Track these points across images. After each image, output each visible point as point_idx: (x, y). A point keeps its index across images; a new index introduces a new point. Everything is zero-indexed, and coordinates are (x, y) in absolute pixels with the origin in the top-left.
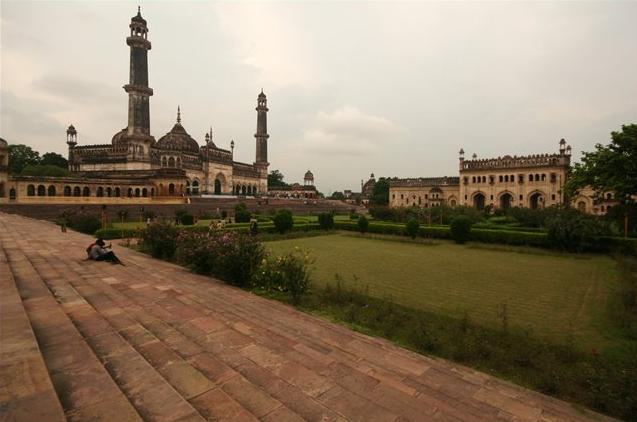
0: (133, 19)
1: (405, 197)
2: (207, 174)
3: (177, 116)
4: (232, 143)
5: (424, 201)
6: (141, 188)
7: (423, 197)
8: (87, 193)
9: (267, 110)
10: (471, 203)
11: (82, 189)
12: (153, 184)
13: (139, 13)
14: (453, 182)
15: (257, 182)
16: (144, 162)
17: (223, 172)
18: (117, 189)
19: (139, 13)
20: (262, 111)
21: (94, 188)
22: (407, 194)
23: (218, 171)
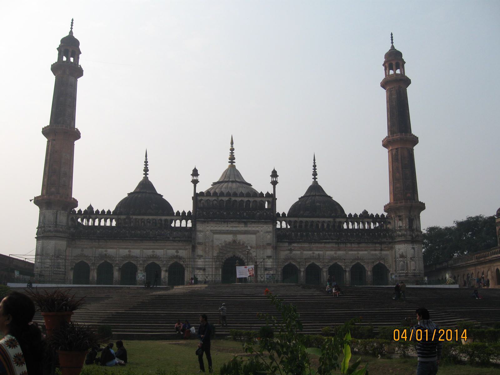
2: (194, 248)
3: (228, 155)
4: (274, 174)
13: (71, 32)
17: (240, 237)
19: (71, 32)
23: (229, 238)
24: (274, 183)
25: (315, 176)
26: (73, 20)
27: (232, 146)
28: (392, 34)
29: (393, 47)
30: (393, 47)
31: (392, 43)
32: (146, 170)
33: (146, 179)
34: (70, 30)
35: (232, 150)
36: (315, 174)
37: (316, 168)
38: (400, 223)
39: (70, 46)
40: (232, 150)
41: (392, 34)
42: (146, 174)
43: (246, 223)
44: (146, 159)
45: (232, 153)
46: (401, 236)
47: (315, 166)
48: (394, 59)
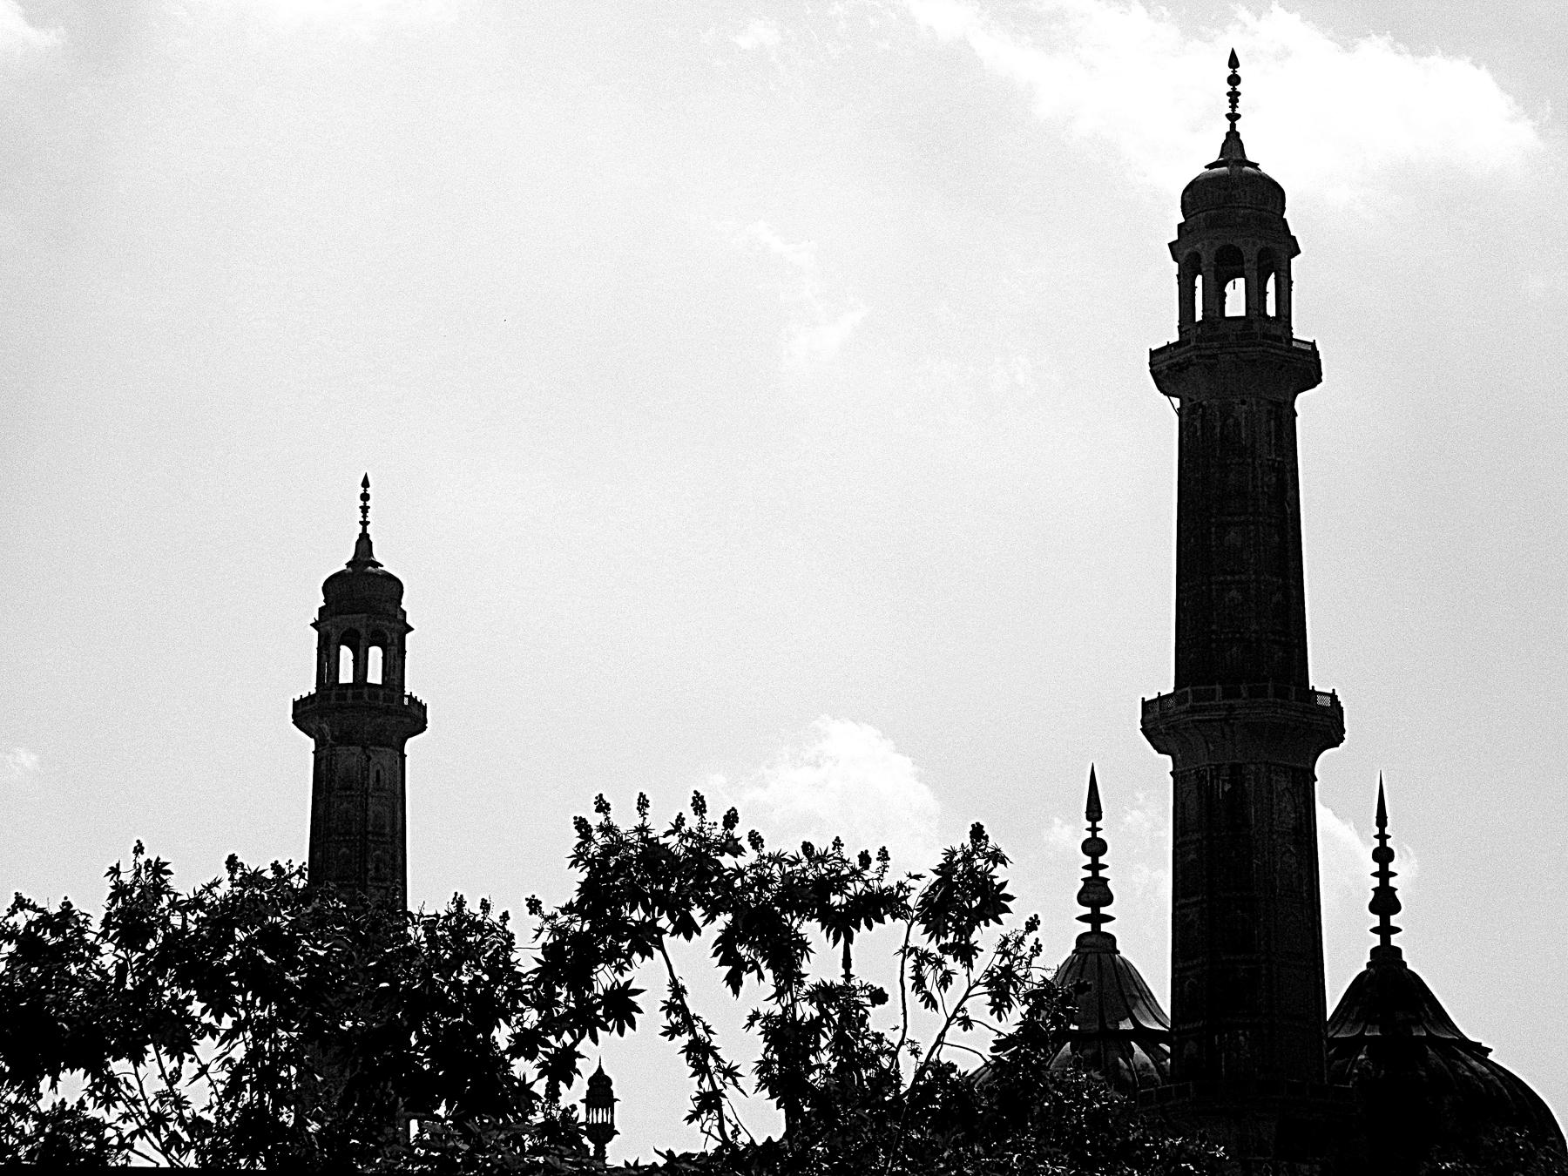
13: (364, 542)
19: (364, 542)
25: (1385, 921)
26: (365, 484)
27: (1094, 830)
28: (1234, 62)
29: (1233, 141)
30: (1233, 141)
31: (1233, 117)
34: (359, 529)
35: (1094, 847)
37: (1392, 867)
39: (362, 604)
40: (1094, 847)
41: (1234, 62)
45: (1095, 867)
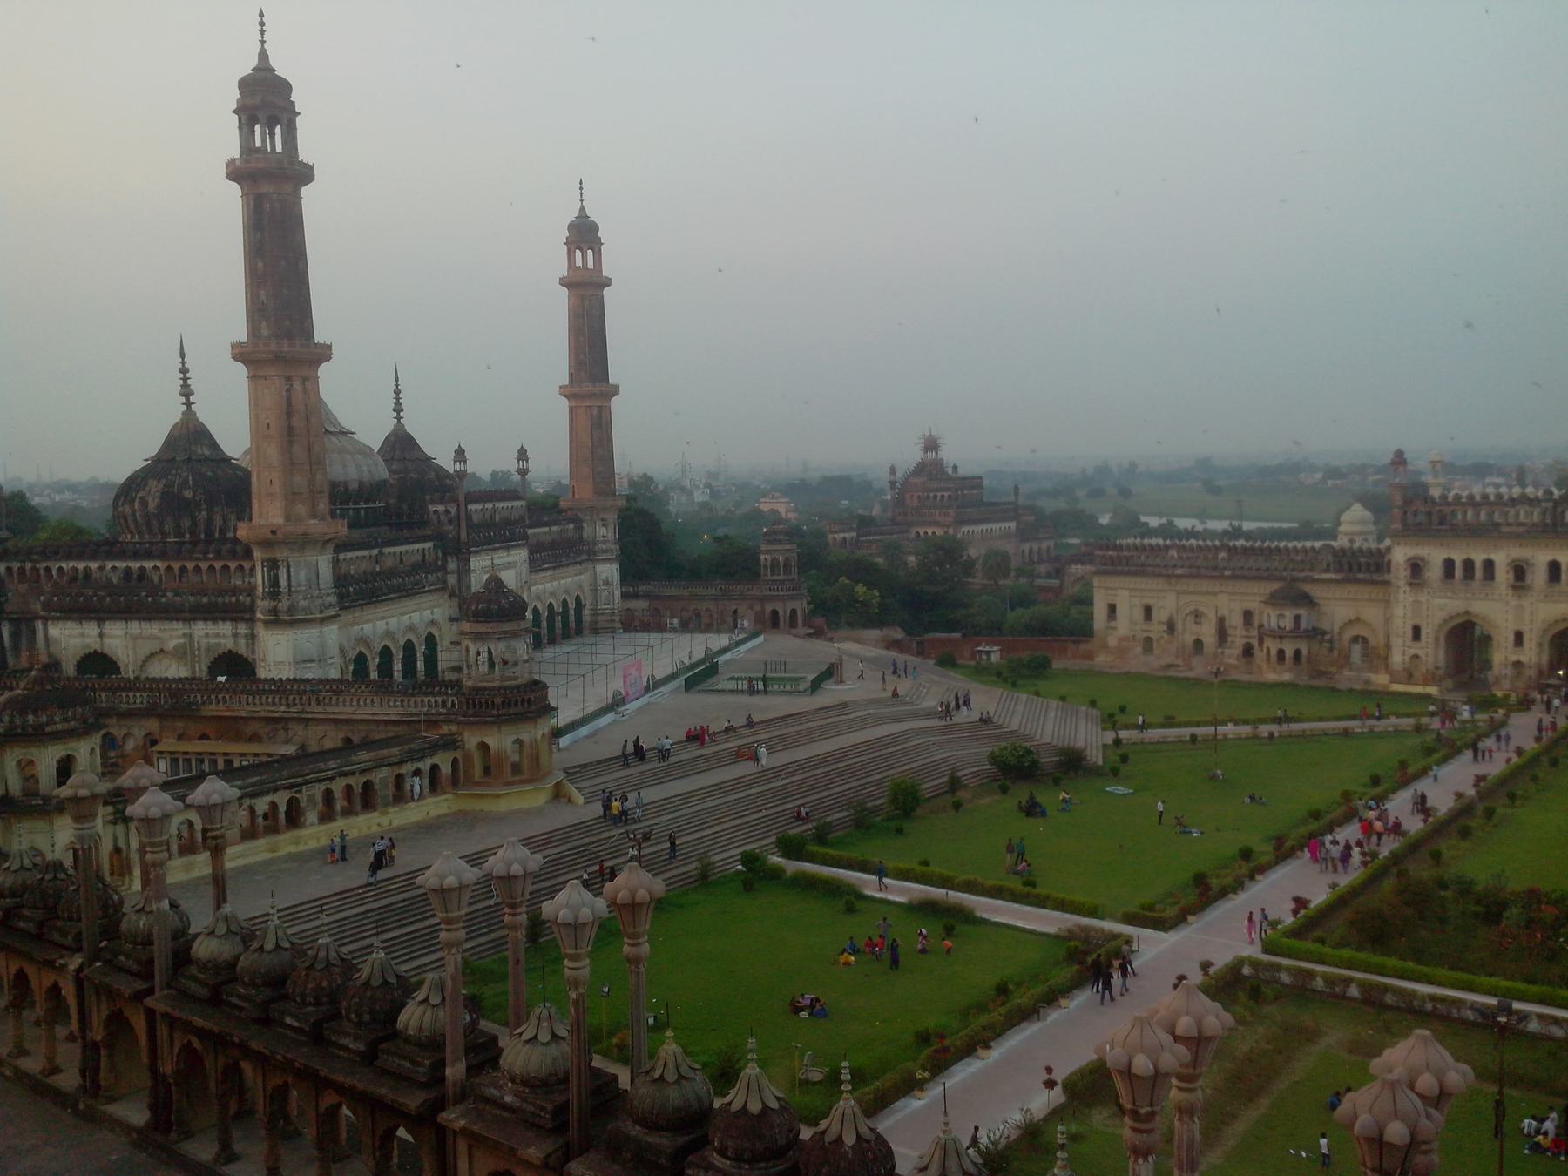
0: (245, 84)
1: (1160, 615)
4: (522, 455)
5: (1238, 638)
6: (425, 765)
7: (1235, 620)
8: (294, 818)
9: (607, 283)
10: (1432, 653)
11: (283, 809)
12: (450, 743)
13: (263, 55)
14: (1364, 568)
15: (585, 578)
16: (323, 621)
18: (368, 786)
19: (263, 55)
20: (587, 294)
21: (311, 799)
22: (1168, 603)
24: (523, 472)
26: (261, 15)
29: (582, 209)
30: (582, 209)
32: (186, 392)
33: (189, 413)
36: (398, 409)
38: (602, 531)
42: (189, 404)
43: (508, 548)
44: (183, 363)
46: (607, 551)
47: (397, 392)
48: (584, 234)
